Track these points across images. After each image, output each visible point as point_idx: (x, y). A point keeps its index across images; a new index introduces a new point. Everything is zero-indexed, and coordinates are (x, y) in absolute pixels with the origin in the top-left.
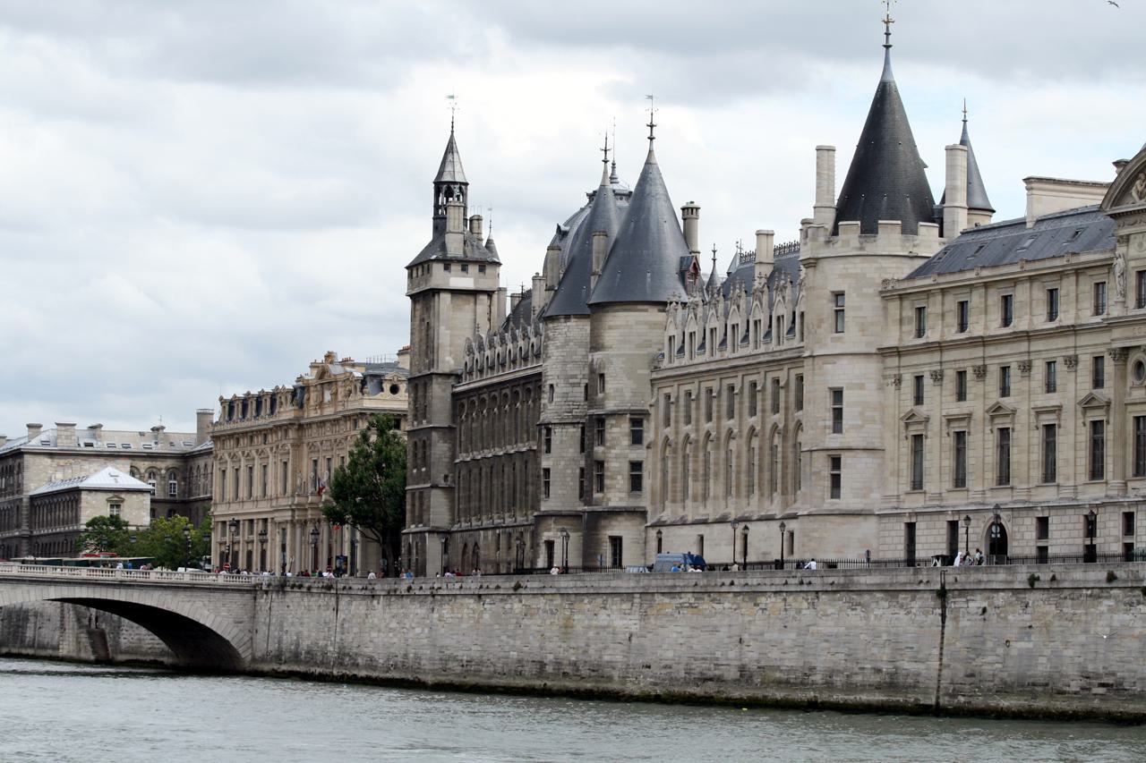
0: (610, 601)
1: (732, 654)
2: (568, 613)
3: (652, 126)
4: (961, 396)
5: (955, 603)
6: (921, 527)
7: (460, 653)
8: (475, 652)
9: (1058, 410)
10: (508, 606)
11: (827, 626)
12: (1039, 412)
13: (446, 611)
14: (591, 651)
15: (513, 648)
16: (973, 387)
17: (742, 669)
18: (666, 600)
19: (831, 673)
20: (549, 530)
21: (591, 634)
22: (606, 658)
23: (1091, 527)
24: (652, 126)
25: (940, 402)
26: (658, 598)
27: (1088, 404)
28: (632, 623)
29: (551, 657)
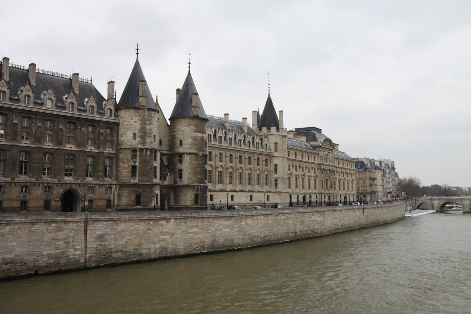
2: (302, 218)
3: (189, 63)
7: (259, 235)
8: (267, 233)
9: (311, 176)
10: (279, 217)
11: (352, 216)
12: (308, 176)
13: (249, 221)
14: (311, 227)
15: (284, 229)
17: (341, 225)
19: (353, 224)
20: (157, 190)
21: (310, 222)
22: (316, 228)
23: (290, 196)
24: (189, 63)
27: (314, 177)
28: (321, 218)
29: (298, 230)
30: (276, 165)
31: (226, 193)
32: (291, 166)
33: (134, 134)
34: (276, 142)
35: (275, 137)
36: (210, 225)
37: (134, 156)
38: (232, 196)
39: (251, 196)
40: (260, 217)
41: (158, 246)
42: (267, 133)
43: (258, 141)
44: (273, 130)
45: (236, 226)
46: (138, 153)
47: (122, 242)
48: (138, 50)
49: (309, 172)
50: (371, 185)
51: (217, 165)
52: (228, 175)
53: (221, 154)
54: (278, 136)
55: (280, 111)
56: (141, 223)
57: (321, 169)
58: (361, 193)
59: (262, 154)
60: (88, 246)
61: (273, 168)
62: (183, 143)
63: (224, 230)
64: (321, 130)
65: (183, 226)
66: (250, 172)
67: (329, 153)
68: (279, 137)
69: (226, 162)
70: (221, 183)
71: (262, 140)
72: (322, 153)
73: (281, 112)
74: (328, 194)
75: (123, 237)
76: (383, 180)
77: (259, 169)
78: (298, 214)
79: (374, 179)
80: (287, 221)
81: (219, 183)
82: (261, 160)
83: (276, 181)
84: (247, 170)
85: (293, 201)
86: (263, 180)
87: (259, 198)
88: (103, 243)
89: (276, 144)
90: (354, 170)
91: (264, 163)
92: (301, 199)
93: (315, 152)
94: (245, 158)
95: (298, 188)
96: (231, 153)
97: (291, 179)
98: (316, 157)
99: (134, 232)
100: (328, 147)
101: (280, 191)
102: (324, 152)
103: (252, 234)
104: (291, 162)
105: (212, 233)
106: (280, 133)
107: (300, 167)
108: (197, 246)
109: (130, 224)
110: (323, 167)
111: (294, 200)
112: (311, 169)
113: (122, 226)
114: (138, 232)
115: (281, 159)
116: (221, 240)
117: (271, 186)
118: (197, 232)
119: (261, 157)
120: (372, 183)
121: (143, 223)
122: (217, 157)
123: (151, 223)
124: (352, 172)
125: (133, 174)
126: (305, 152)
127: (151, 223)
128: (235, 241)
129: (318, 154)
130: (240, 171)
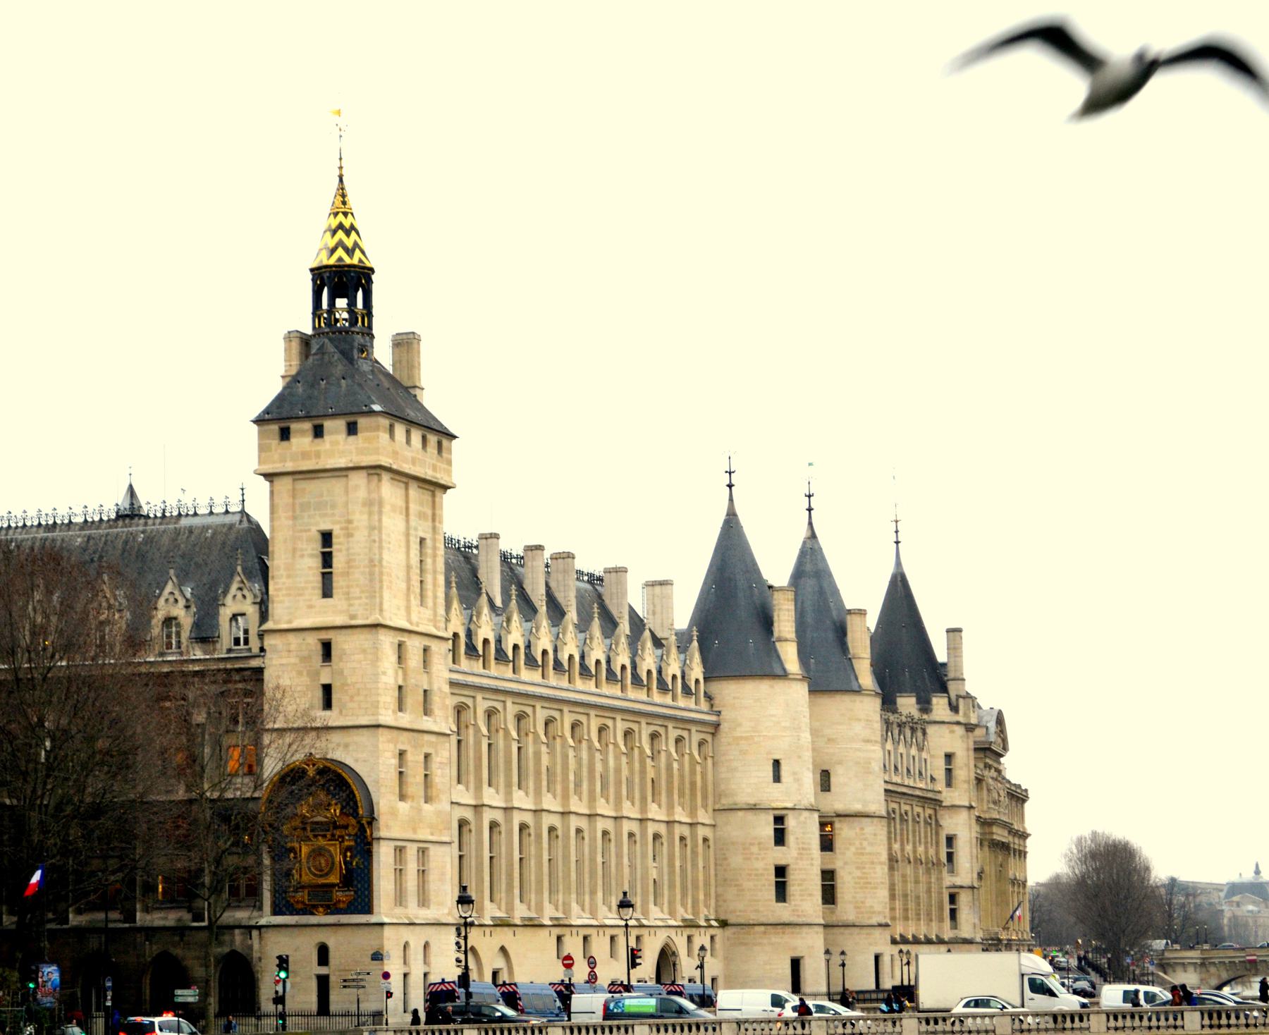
3: (809, 496)
30: (950, 840)
33: (777, 763)
34: (949, 750)
35: (944, 728)
37: (780, 837)
42: (916, 714)
46: (791, 823)
54: (956, 728)
55: (948, 631)
59: (924, 800)
61: (944, 850)
62: (833, 779)
68: (960, 730)
73: (954, 632)
83: (953, 898)
106: (960, 718)
117: (941, 920)
125: (781, 892)
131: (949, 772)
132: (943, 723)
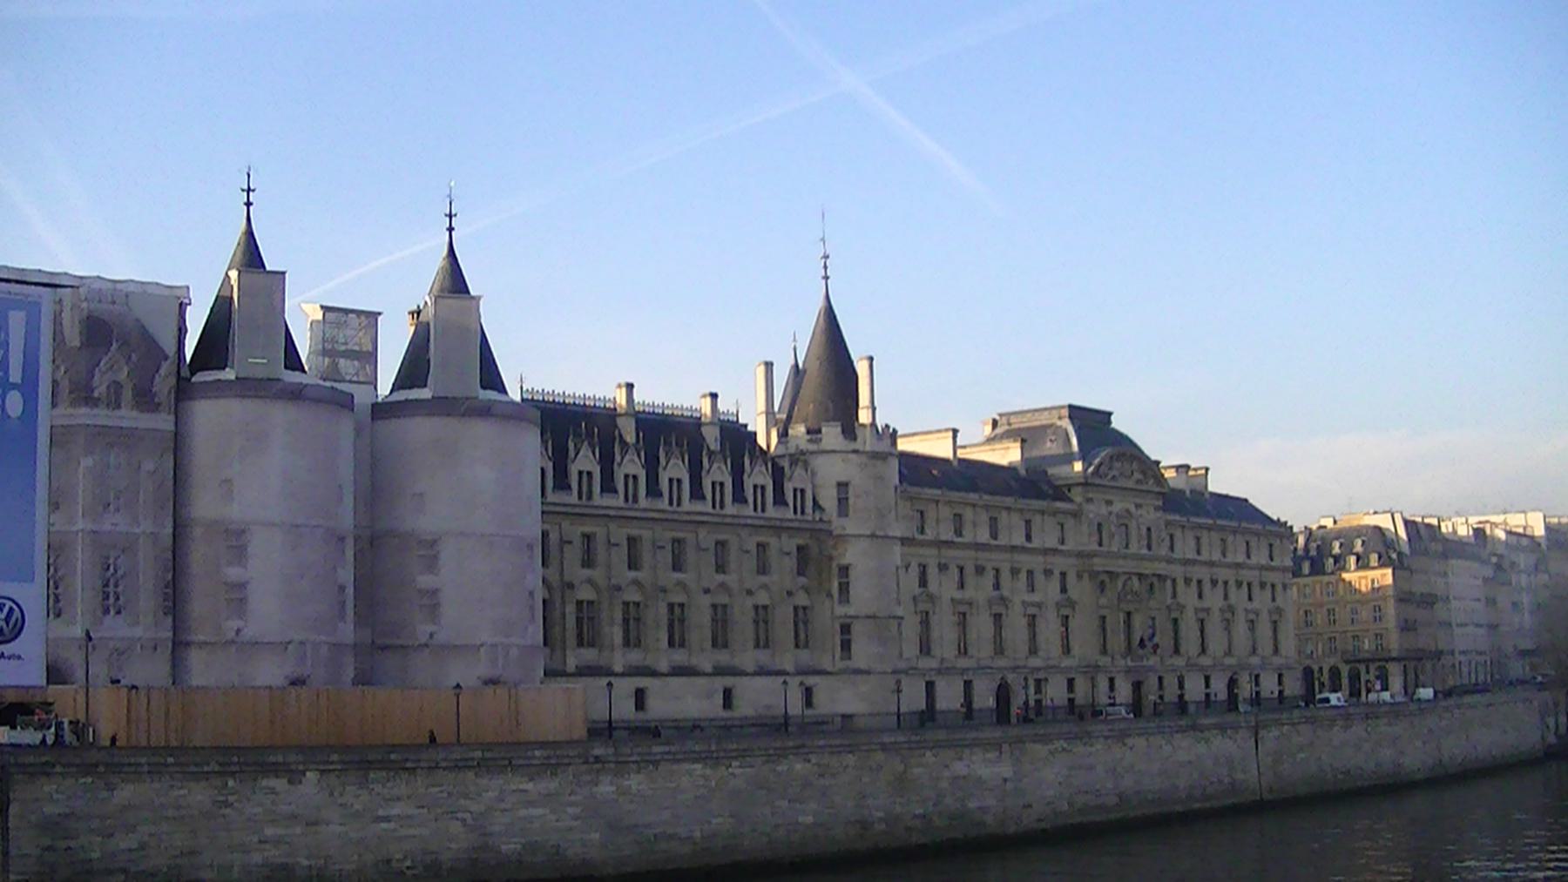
0: (967, 751)
1: (1109, 785)
4: (962, 586)
5: (1262, 733)
6: (941, 686)
7: (682, 831)
9: (1039, 605)
13: (635, 782)
14: (948, 800)
16: (970, 580)
17: (1120, 796)
18: (1038, 746)
25: (944, 587)
26: (1029, 746)
27: (1058, 605)
29: (880, 814)
30: (845, 570)
31: (604, 681)
32: (932, 572)
34: (843, 479)
35: (837, 458)
36: (466, 796)
38: (640, 695)
39: (728, 694)
40: (686, 766)
41: (257, 858)
43: (760, 481)
44: (832, 435)
45: (573, 798)
47: (124, 842)
48: (249, 190)
49: (1032, 588)
50: (1407, 627)
51: (567, 578)
52: (619, 616)
53: (588, 537)
56: (192, 784)
57: (1093, 575)
58: (1367, 661)
59: (778, 529)
60: (13, 852)
63: (523, 812)
64: (1110, 414)
65: (356, 797)
66: (723, 599)
67: (1138, 506)
69: (609, 567)
70: (592, 645)
71: (778, 475)
72: (1096, 510)
74: (1128, 671)
75: (132, 829)
76: (1491, 602)
77: (765, 587)
78: (880, 756)
79: (1429, 601)
80: (822, 781)
81: (580, 644)
82: (773, 553)
84: (707, 591)
85: (941, 704)
86: (783, 629)
87: (758, 696)
88: (62, 844)
89: (842, 486)
90: (1284, 570)
91: (790, 563)
92: (985, 699)
93: (1059, 505)
94: (699, 548)
95: (971, 651)
96: (635, 532)
97: (934, 620)
98: (1070, 523)
99: (170, 813)
100: (1130, 484)
101: (863, 665)
102: (1109, 503)
103: (648, 826)
104: (934, 551)
105: (470, 821)
106: (858, 445)
107: (980, 570)
108: (408, 863)
109: (156, 785)
110: (1099, 564)
111: (949, 697)
112: (1039, 578)
113: (126, 793)
114: (184, 812)
115: (864, 544)
116: (510, 846)
118: (409, 817)
119: (773, 541)
120: (1421, 614)
121: (203, 784)
122: (567, 548)
123: (231, 783)
124: (1271, 577)
126: (1008, 509)
127: (231, 783)
128: (570, 853)
129: (1076, 515)
130: (678, 598)
131: (843, 502)
132: (834, 451)
